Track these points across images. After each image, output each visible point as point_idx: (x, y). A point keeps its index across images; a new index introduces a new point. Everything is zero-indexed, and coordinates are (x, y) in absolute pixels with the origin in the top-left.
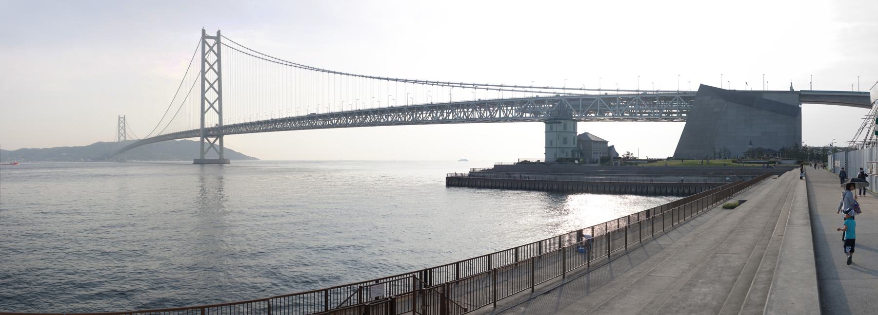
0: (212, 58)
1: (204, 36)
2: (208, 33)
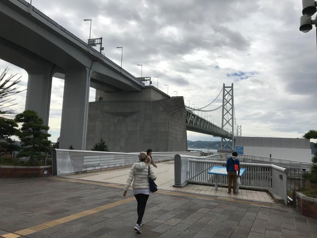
0: (228, 97)
1: (224, 87)
2: (225, 86)
